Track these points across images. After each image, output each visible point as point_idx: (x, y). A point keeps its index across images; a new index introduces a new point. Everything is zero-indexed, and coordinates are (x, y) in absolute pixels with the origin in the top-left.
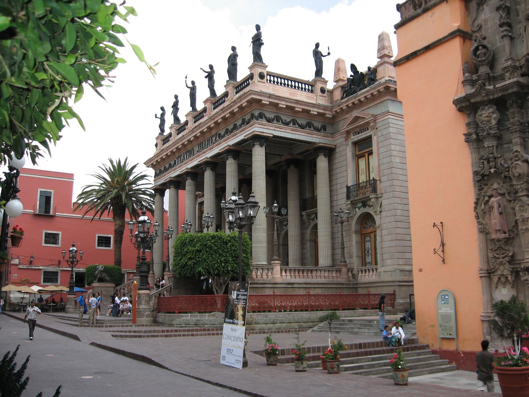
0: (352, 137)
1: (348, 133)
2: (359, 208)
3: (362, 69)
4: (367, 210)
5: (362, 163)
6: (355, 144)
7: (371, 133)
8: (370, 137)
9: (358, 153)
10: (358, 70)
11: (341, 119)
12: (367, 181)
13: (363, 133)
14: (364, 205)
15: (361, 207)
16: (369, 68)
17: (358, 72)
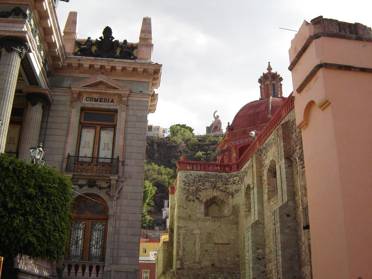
0: (84, 101)
1: (80, 94)
2: (81, 186)
3: (118, 36)
4: (94, 191)
5: (88, 135)
6: (83, 109)
7: (117, 107)
8: (116, 111)
9: (82, 121)
10: (113, 35)
11: (68, 75)
12: (93, 157)
13: (104, 103)
14: (92, 184)
15: (84, 185)
16: (125, 41)
17: (113, 38)
